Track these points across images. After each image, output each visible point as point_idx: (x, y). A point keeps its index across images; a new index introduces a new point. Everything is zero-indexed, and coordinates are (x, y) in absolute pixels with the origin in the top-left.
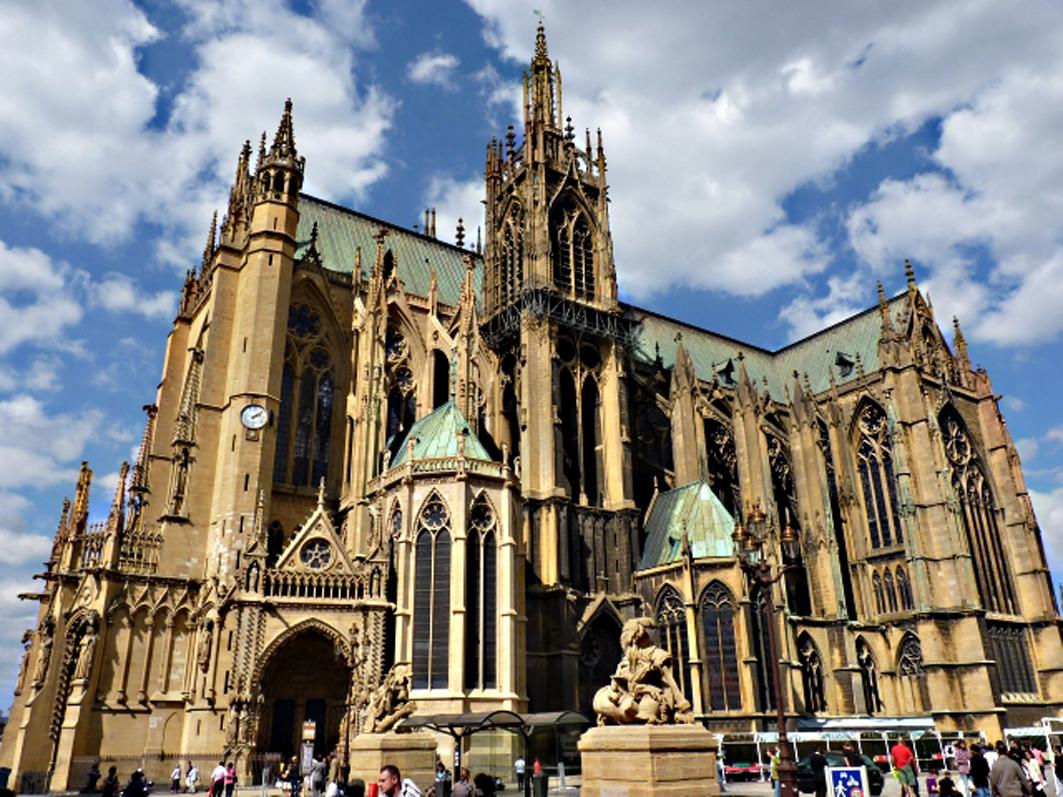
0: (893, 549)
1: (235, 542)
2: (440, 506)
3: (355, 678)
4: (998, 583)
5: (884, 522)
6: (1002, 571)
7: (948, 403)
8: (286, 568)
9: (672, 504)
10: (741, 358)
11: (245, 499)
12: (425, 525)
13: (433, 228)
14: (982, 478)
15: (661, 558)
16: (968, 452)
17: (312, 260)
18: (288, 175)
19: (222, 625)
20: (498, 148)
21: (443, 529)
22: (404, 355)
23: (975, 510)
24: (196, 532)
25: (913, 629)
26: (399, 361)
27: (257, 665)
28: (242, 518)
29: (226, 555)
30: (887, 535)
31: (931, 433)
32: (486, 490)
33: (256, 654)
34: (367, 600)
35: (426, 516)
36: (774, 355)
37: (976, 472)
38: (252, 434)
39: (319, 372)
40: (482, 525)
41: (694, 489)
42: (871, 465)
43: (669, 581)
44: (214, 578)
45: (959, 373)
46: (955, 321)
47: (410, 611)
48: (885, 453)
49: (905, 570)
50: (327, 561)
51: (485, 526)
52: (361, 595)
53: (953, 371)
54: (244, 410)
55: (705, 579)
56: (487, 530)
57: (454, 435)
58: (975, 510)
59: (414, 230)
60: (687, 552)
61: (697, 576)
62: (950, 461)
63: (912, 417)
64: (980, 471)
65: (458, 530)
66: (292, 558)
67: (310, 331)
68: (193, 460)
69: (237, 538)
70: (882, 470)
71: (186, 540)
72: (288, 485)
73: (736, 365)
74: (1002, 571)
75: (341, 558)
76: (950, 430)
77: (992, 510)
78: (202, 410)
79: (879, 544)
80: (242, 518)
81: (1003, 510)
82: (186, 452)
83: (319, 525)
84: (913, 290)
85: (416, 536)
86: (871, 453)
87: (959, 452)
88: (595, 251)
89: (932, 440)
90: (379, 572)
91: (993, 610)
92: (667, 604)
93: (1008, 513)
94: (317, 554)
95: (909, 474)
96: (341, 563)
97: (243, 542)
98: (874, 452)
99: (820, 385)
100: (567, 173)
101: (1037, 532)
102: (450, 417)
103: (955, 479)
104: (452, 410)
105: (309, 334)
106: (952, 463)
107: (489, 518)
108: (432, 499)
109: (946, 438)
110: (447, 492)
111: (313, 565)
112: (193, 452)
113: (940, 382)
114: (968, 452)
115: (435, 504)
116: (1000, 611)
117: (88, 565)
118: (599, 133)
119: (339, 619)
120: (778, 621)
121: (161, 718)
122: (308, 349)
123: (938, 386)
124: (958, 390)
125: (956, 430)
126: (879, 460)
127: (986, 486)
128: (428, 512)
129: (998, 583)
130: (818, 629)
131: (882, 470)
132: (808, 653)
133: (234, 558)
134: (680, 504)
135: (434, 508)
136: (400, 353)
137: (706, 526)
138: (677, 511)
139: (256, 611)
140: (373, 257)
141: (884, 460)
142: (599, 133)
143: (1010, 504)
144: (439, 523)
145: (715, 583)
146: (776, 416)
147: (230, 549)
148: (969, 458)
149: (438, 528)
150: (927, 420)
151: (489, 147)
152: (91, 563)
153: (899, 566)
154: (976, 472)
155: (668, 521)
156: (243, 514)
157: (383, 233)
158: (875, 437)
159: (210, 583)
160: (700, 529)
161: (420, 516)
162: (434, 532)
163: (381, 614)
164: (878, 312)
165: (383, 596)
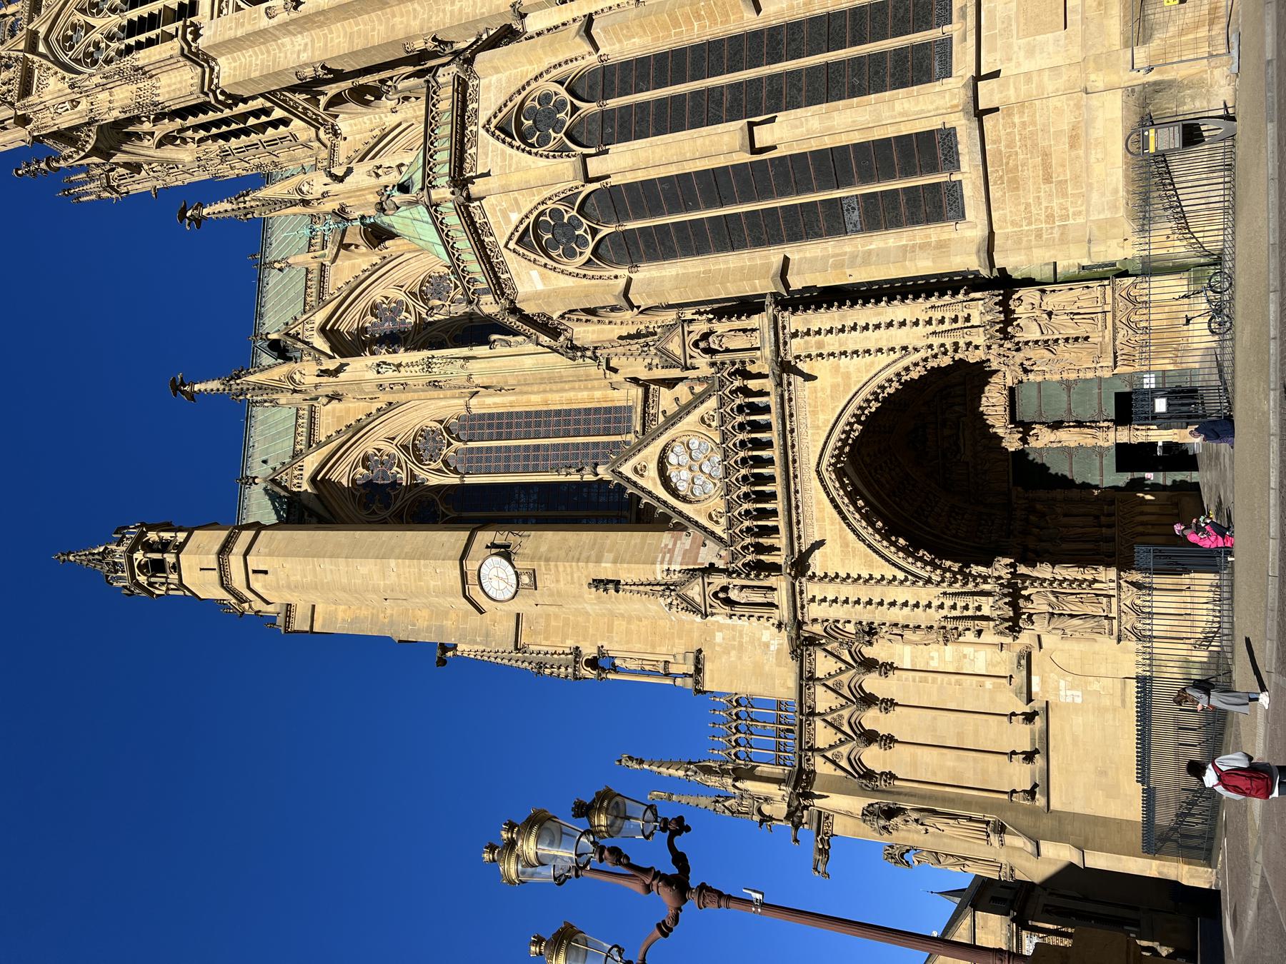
3: (945, 361)
12: (588, 252)
22: (401, 296)
24: (719, 637)
27: (929, 581)
32: (482, 120)
35: (570, 254)
38: (525, 579)
40: (561, 116)
47: (774, 256)
56: (568, 97)
66: (704, 521)
71: (733, 653)
78: (524, 640)
82: (593, 663)
83: (636, 470)
105: (395, 469)
107: (545, 98)
112: (589, 651)
115: (538, 238)
119: (814, 413)
121: (1062, 683)
136: (399, 303)
139: (813, 589)
163: (796, 321)
165: (755, 321)
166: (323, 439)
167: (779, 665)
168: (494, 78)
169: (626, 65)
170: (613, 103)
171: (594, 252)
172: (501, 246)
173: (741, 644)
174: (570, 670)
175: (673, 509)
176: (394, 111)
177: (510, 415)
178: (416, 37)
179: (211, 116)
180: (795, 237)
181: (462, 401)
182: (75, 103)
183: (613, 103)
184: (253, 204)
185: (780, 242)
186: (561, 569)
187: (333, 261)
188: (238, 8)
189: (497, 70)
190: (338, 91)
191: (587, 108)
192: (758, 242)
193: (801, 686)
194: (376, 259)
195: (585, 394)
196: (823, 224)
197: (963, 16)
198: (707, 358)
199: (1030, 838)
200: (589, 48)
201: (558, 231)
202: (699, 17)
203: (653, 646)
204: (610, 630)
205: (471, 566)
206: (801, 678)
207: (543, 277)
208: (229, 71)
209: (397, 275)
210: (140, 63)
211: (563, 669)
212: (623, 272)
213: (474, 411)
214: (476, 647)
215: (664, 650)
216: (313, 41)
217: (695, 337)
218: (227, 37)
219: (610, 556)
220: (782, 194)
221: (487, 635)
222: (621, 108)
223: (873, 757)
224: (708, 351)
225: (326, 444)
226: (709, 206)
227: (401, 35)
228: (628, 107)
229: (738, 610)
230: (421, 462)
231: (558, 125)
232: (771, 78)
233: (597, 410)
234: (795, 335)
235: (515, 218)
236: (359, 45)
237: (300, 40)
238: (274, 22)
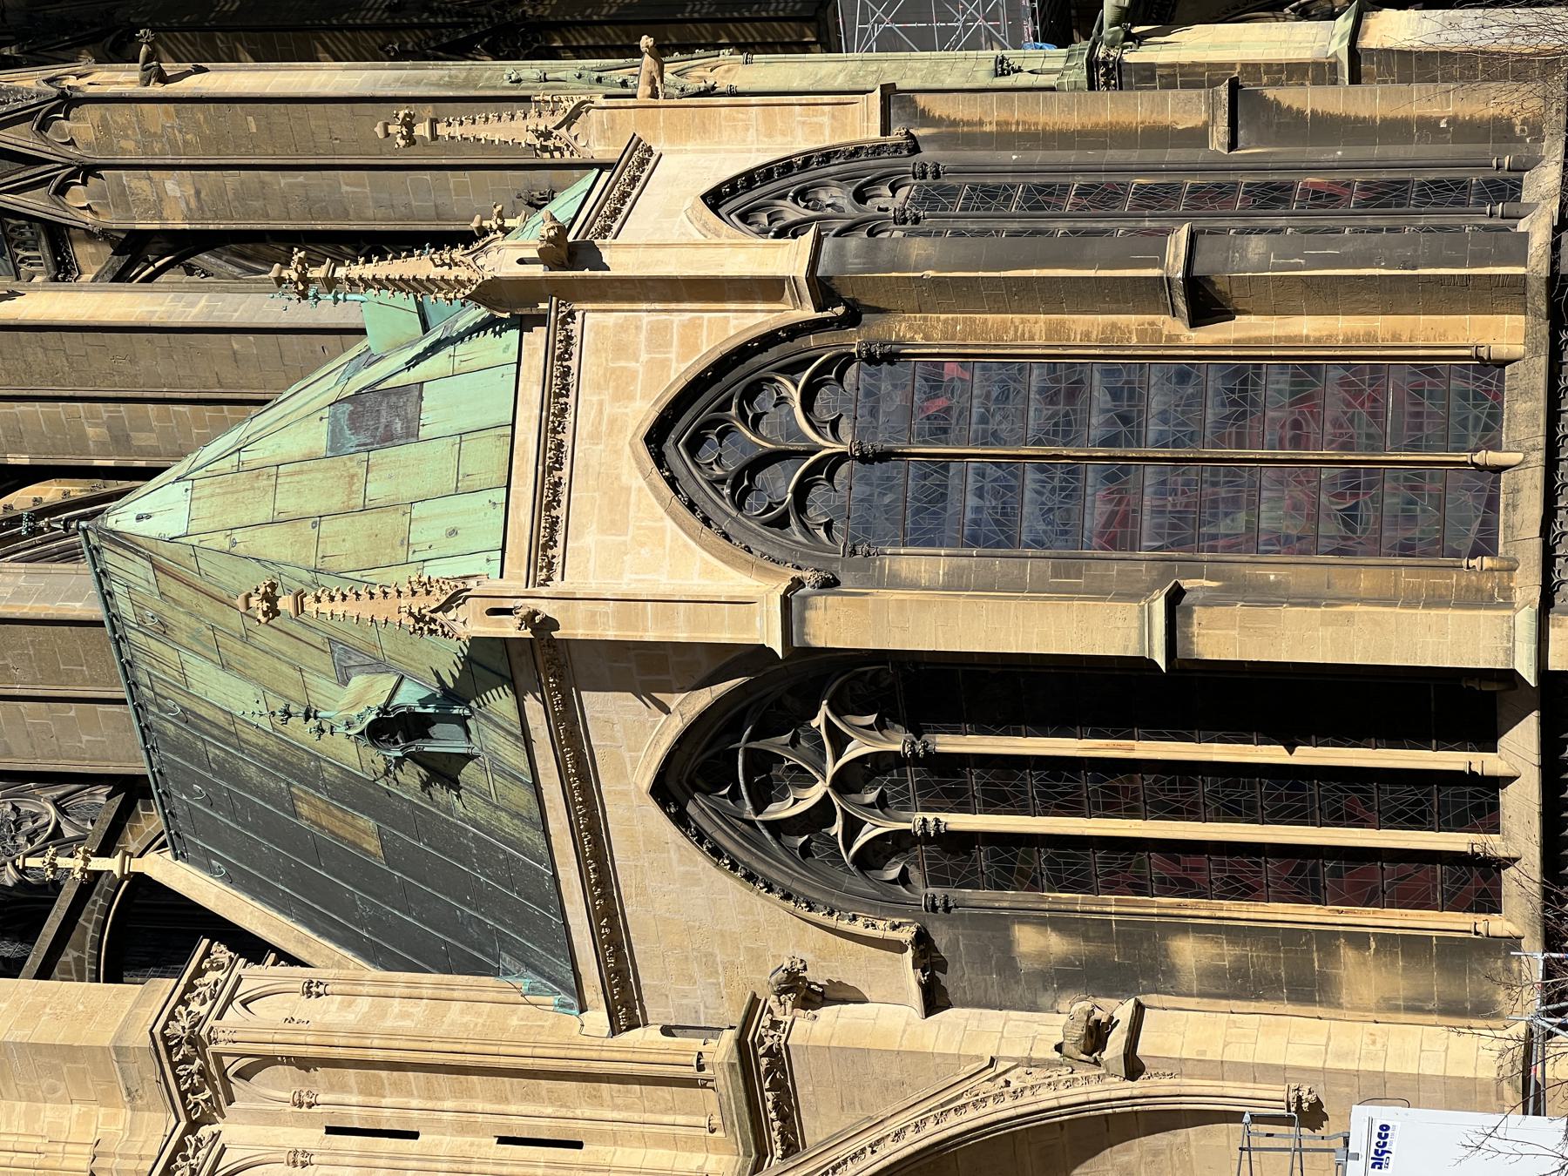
92: (782, 810)
137: (336, 503)
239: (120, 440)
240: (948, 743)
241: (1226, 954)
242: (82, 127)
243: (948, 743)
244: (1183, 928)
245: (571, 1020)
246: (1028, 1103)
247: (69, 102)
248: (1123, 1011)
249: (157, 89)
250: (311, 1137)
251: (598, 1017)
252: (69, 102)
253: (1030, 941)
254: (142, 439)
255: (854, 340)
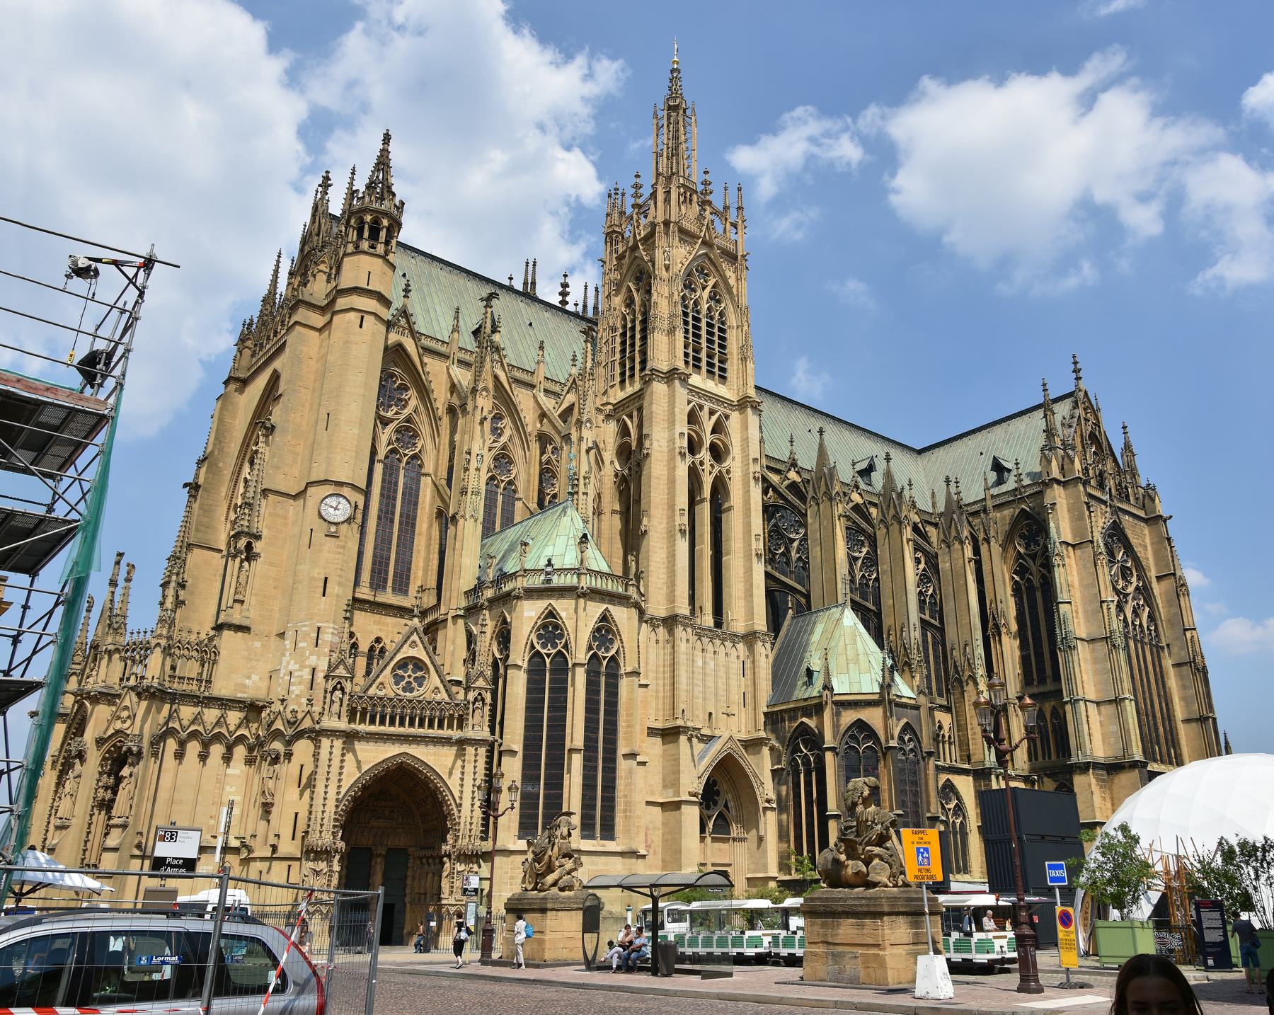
0: (1049, 687)
1: (308, 658)
2: (557, 627)
4: (1161, 729)
5: (1039, 655)
6: (1166, 716)
7: (1115, 521)
8: (372, 692)
9: (809, 628)
10: (888, 459)
11: (322, 606)
12: (538, 647)
13: (534, 283)
14: (1147, 609)
15: (796, 692)
16: (1134, 579)
17: (403, 322)
18: (385, 222)
19: (289, 755)
20: (619, 196)
21: (560, 651)
22: (503, 439)
23: (1139, 646)
24: (258, 644)
25: (1066, 780)
26: (498, 445)
27: (337, 807)
28: (319, 629)
29: (297, 674)
30: (1041, 670)
31: (1096, 556)
33: (338, 793)
34: (468, 733)
35: (539, 637)
36: (920, 452)
37: (1141, 603)
39: (405, 455)
41: (835, 612)
42: (1027, 588)
43: (804, 719)
44: (283, 701)
45: (1126, 488)
46: (1124, 427)
47: (518, 746)
48: (1043, 576)
49: (1061, 712)
50: (420, 685)
51: (607, 650)
52: (460, 727)
53: (1120, 484)
54: (326, 497)
55: (849, 717)
56: (609, 655)
57: (571, 542)
58: (1139, 646)
59: (507, 283)
60: (828, 687)
61: (838, 714)
62: (1114, 588)
63: (1074, 535)
64: (1145, 600)
65: (580, 654)
66: (378, 681)
67: (397, 406)
68: (258, 555)
69: (311, 654)
70: (1039, 595)
71: (246, 653)
72: (367, 590)
73: (881, 465)
74: (1166, 716)
75: (438, 682)
76: (1116, 552)
77: (1157, 646)
78: (271, 497)
79: (1033, 680)
80: (319, 629)
81: (1168, 645)
82: (249, 547)
84: (1080, 390)
85: (527, 659)
86: (1027, 575)
87: (1124, 578)
88: (729, 327)
89: (1096, 565)
90: (483, 700)
91: (1155, 761)
93: (1175, 649)
94: (409, 676)
95: (1070, 603)
96: (437, 688)
97: (318, 659)
98: (1031, 574)
99: (972, 492)
100: (702, 234)
101: (1204, 672)
102: (566, 520)
103: (1120, 608)
104: (569, 511)
105: (395, 409)
106: (1117, 592)
107: (612, 641)
108: (545, 618)
109: (1112, 561)
110: (564, 610)
111: (404, 689)
112: (258, 547)
113: (1106, 497)
114: (1134, 579)
115: (551, 623)
116: (1162, 762)
117: (128, 679)
118: (740, 189)
119: (435, 754)
120: (926, 769)
122: (392, 426)
123: (1104, 502)
124: (1125, 507)
125: (1121, 553)
126: (1036, 583)
127: (1151, 617)
128: (542, 632)
129: (1161, 729)
130: (963, 778)
131: (1039, 595)
132: (952, 806)
133: (308, 677)
134: (819, 629)
135: (550, 628)
138: (816, 637)
139: (338, 744)
140: (472, 317)
141: (1041, 584)
142: (740, 189)
143: (1177, 639)
144: (554, 645)
145: (860, 725)
146: (920, 525)
147: (302, 667)
148: (1134, 585)
149: (554, 651)
150: (1092, 542)
151: (610, 196)
152: (133, 678)
153: (1054, 707)
154: (1141, 603)
155: (805, 647)
156: (319, 625)
157: (492, 296)
158: (1033, 557)
159: (277, 707)
160: (842, 660)
161: (533, 637)
162: (548, 655)
163: (482, 751)
164: (1040, 413)
165: (487, 729)
166: (426, 360)
167: (236, 685)
168: (625, 616)
169: (616, 686)
170: (603, 679)
171: (538, 651)
172: (551, 602)
173: (251, 660)
174: (246, 530)
175: (388, 663)
176: (612, 462)
177: (416, 504)
178: (649, 521)
179: (637, 367)
180: (525, 757)
181: (431, 472)
182: (667, 268)
183: (603, 679)
184: (587, 385)
185: (524, 750)
186: (337, 556)
187: (534, 397)
188: (689, 402)
189: (629, 618)
190: (632, 434)
191: (605, 663)
192: (526, 739)
193: (223, 699)
194: (529, 429)
195: (421, 564)
196: (529, 773)
197: (604, 846)
198: (472, 700)
199: (121, 844)
200: (629, 669)
201: (552, 635)
202: (628, 726)
203: (256, 595)
204: (271, 564)
205: (346, 491)
206: (227, 700)
207: (531, 618)
208: (659, 388)
209: (516, 438)
210: (677, 332)
211: (246, 524)
212: (525, 665)
213: (423, 478)
214: (267, 454)
215: (253, 602)
216: (662, 452)
217: (483, 693)
218: (677, 400)
219: (340, 593)
220: (547, 755)
221: (277, 468)
222: (600, 681)
223: (171, 745)
224: (476, 700)
225: (421, 361)
226: (548, 717)
227: (653, 512)
228: (599, 685)
229: (328, 695)
230: (396, 431)
231: (599, 648)
232: (597, 758)
233: (409, 570)
234: (476, 749)
235: (563, 615)
236: (654, 483)
237: (664, 444)
238: (677, 435)
239: (884, 572)
240: (814, 774)
241: (785, 824)
242: (957, 546)
243: (814, 774)
244: (788, 816)
245: (764, 704)
246: (757, 790)
247: (962, 543)
248: (774, 806)
249: (967, 561)
250: (742, 658)
251: (766, 710)
252: (962, 543)
253: (784, 788)
254: (885, 577)
255: (880, 754)
